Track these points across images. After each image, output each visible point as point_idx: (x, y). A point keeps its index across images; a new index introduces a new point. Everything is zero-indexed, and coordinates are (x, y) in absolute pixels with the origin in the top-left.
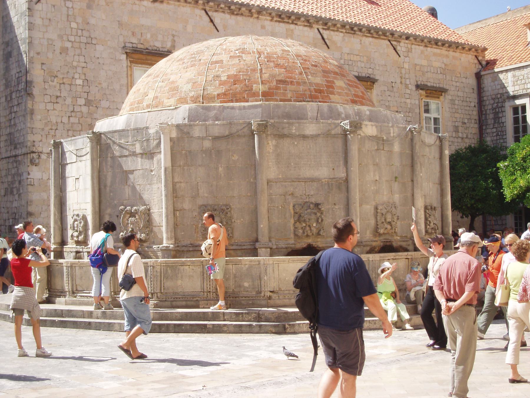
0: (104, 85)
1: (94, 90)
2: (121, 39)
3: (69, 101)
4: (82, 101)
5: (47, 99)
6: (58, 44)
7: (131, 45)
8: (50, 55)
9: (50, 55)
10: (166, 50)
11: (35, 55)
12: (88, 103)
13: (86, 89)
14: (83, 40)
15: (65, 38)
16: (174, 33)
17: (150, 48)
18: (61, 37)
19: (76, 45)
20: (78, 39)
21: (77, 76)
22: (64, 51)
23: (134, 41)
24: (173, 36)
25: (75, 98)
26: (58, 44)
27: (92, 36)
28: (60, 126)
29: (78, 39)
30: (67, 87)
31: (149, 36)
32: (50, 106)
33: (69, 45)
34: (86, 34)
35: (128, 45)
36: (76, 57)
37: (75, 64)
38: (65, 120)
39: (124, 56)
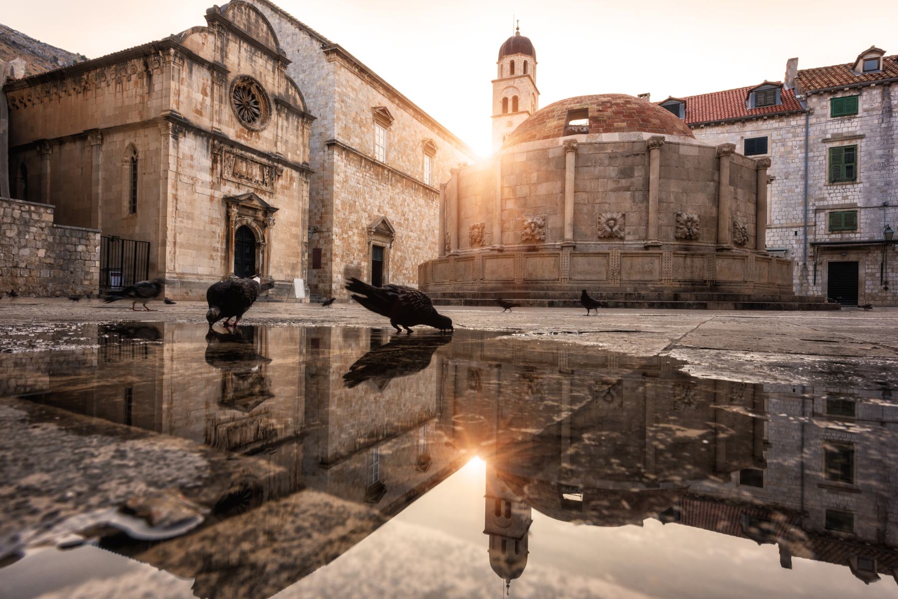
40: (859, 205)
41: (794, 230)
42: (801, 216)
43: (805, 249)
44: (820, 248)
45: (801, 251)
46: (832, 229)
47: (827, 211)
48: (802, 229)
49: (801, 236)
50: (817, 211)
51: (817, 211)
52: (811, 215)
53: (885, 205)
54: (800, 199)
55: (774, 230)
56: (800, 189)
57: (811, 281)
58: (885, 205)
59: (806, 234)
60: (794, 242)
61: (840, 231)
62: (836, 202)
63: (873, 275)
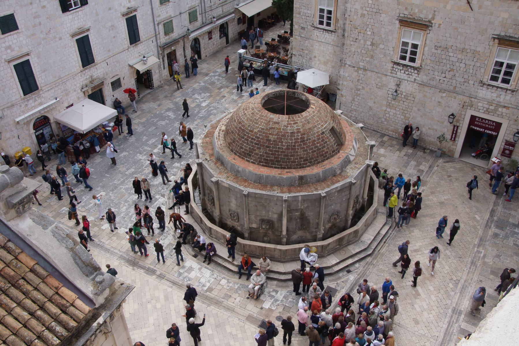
0: (383, 36)
1: (377, 38)
2: (398, 11)
3: (362, 42)
4: (369, 43)
5: (351, 39)
6: (360, 11)
7: (403, 15)
8: (355, 17)
9: (355, 17)
10: (427, 20)
11: (348, 17)
12: (372, 44)
13: (373, 37)
14: (375, 10)
15: (364, 8)
16: (436, 9)
17: (416, 18)
18: (362, 8)
19: (370, 13)
20: (371, 10)
21: (368, 30)
22: (363, 15)
23: (406, 13)
24: (435, 11)
25: (365, 41)
26: (360, 11)
27: (380, 8)
28: (356, 53)
29: (371, 10)
30: (362, 34)
31: (416, 11)
32: (352, 43)
33: (366, 12)
34: (376, 7)
35: (401, 15)
36: (369, 20)
37: (368, 23)
38: (359, 50)
39: (397, 22)
40: (173, 16)
41: (152, 39)
42: (153, 29)
43: (158, 49)
44: (163, 48)
45: (156, 51)
46: (166, 34)
47: (162, 23)
48: (154, 38)
49: (155, 43)
50: (158, 24)
51: (158, 24)
52: (157, 27)
53: (180, 14)
54: (152, 19)
55: (144, 43)
56: (150, 12)
57: (162, 68)
58: (180, 14)
59: (157, 41)
60: (152, 47)
61: (168, 34)
62: (164, 17)
63: (181, 54)
